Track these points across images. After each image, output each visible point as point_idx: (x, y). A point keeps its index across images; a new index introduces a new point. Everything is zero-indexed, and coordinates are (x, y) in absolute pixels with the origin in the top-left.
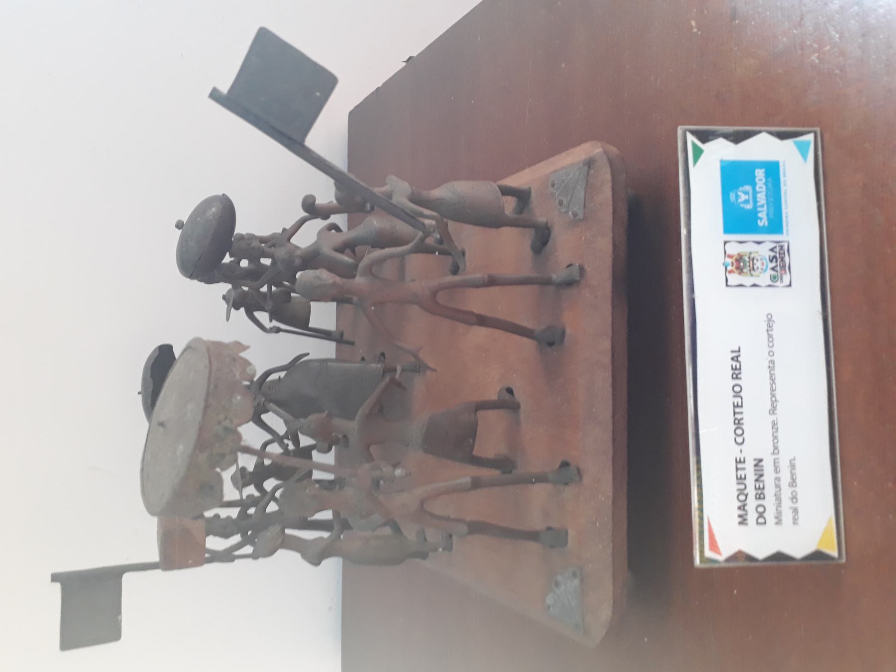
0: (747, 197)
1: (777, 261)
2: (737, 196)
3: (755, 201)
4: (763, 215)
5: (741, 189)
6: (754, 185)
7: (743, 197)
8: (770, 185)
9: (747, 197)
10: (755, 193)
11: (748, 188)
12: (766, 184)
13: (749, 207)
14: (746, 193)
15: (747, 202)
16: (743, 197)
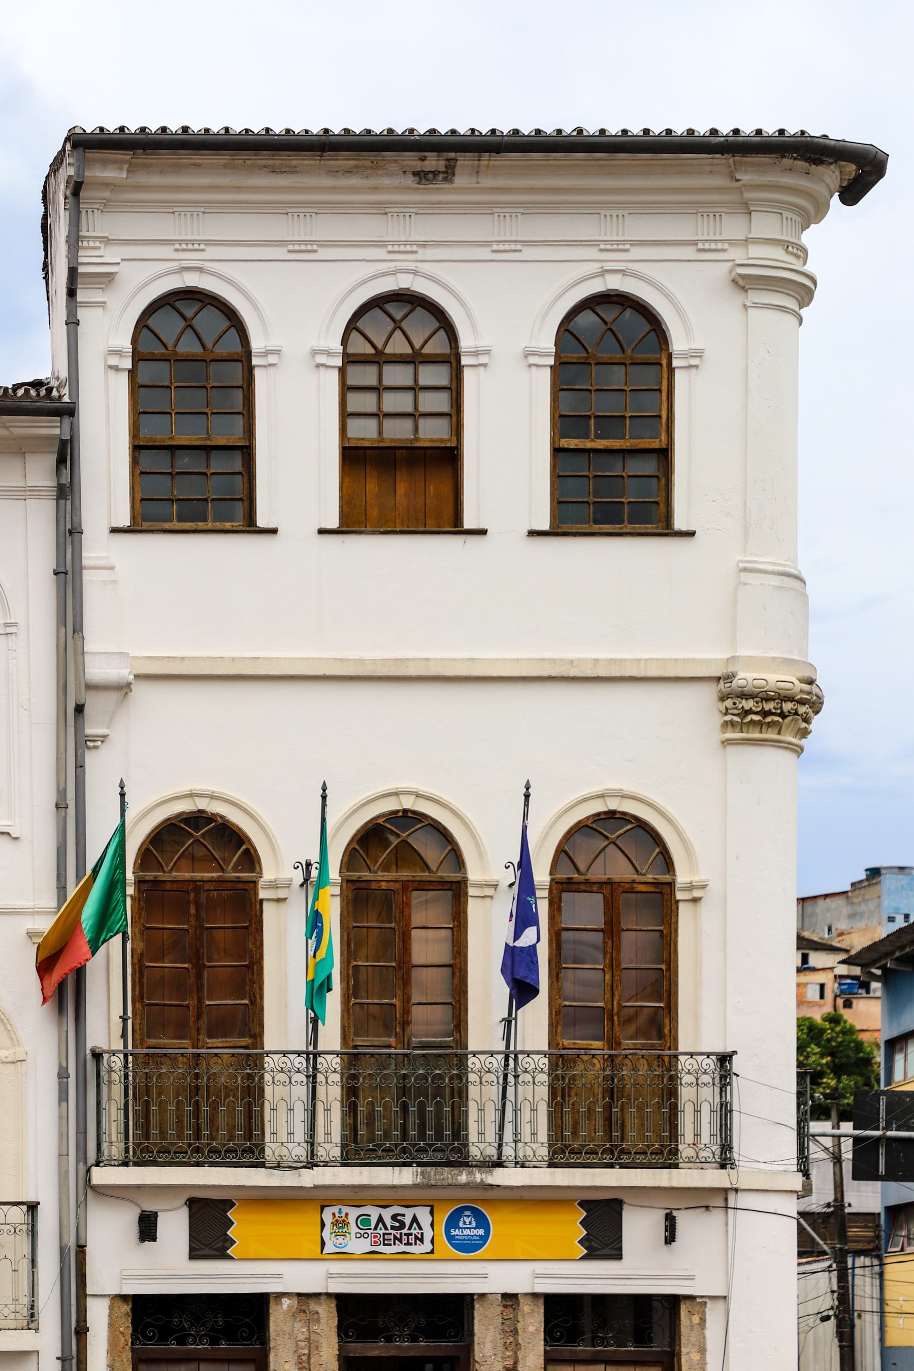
0: (467, 1223)
1: (393, 1228)
2: (469, 1216)
3: (465, 1228)
4: (457, 1232)
5: (473, 1219)
6: (475, 1228)
7: (467, 1221)
8: (475, 1238)
9: (467, 1223)
10: (470, 1229)
11: (474, 1225)
12: (475, 1235)
13: (461, 1224)
14: (470, 1223)
15: (465, 1223)
16: (467, 1221)
